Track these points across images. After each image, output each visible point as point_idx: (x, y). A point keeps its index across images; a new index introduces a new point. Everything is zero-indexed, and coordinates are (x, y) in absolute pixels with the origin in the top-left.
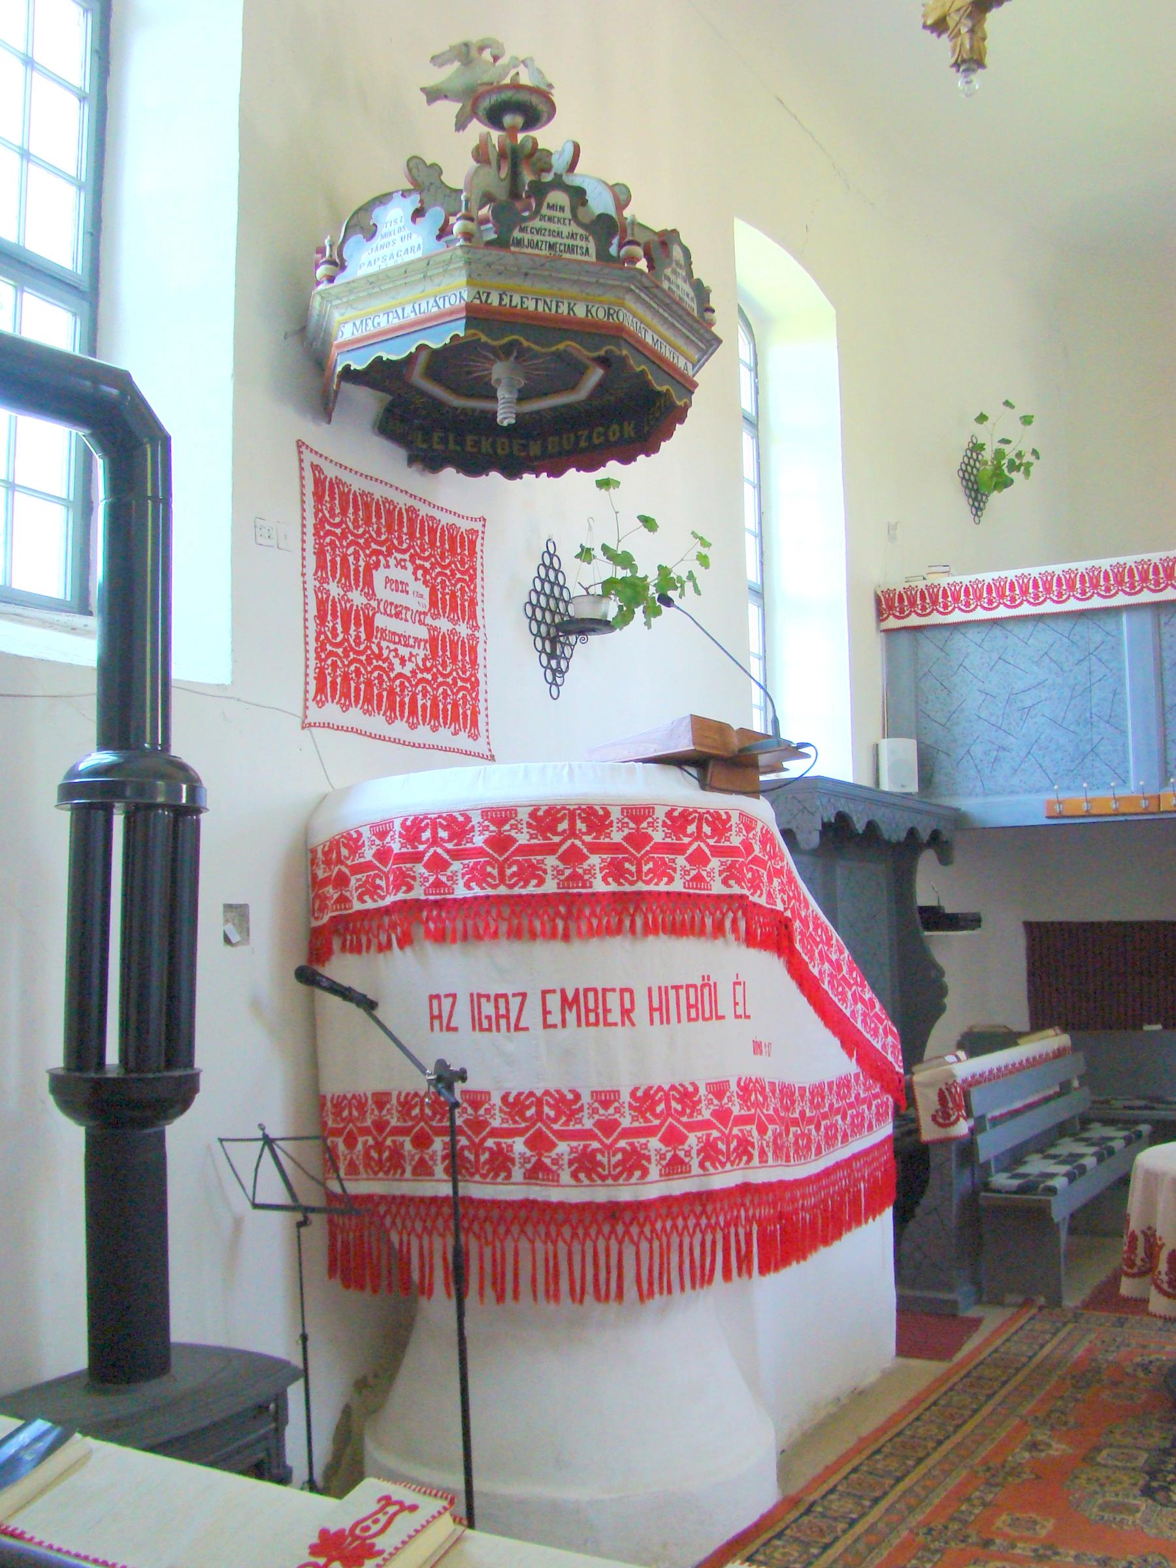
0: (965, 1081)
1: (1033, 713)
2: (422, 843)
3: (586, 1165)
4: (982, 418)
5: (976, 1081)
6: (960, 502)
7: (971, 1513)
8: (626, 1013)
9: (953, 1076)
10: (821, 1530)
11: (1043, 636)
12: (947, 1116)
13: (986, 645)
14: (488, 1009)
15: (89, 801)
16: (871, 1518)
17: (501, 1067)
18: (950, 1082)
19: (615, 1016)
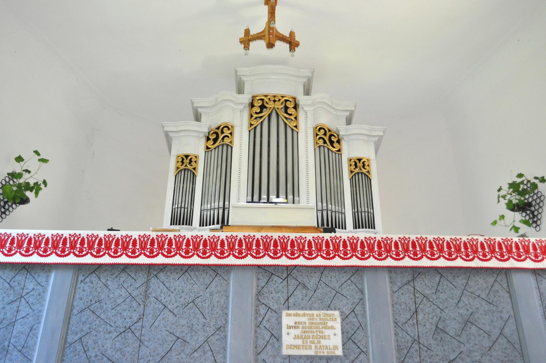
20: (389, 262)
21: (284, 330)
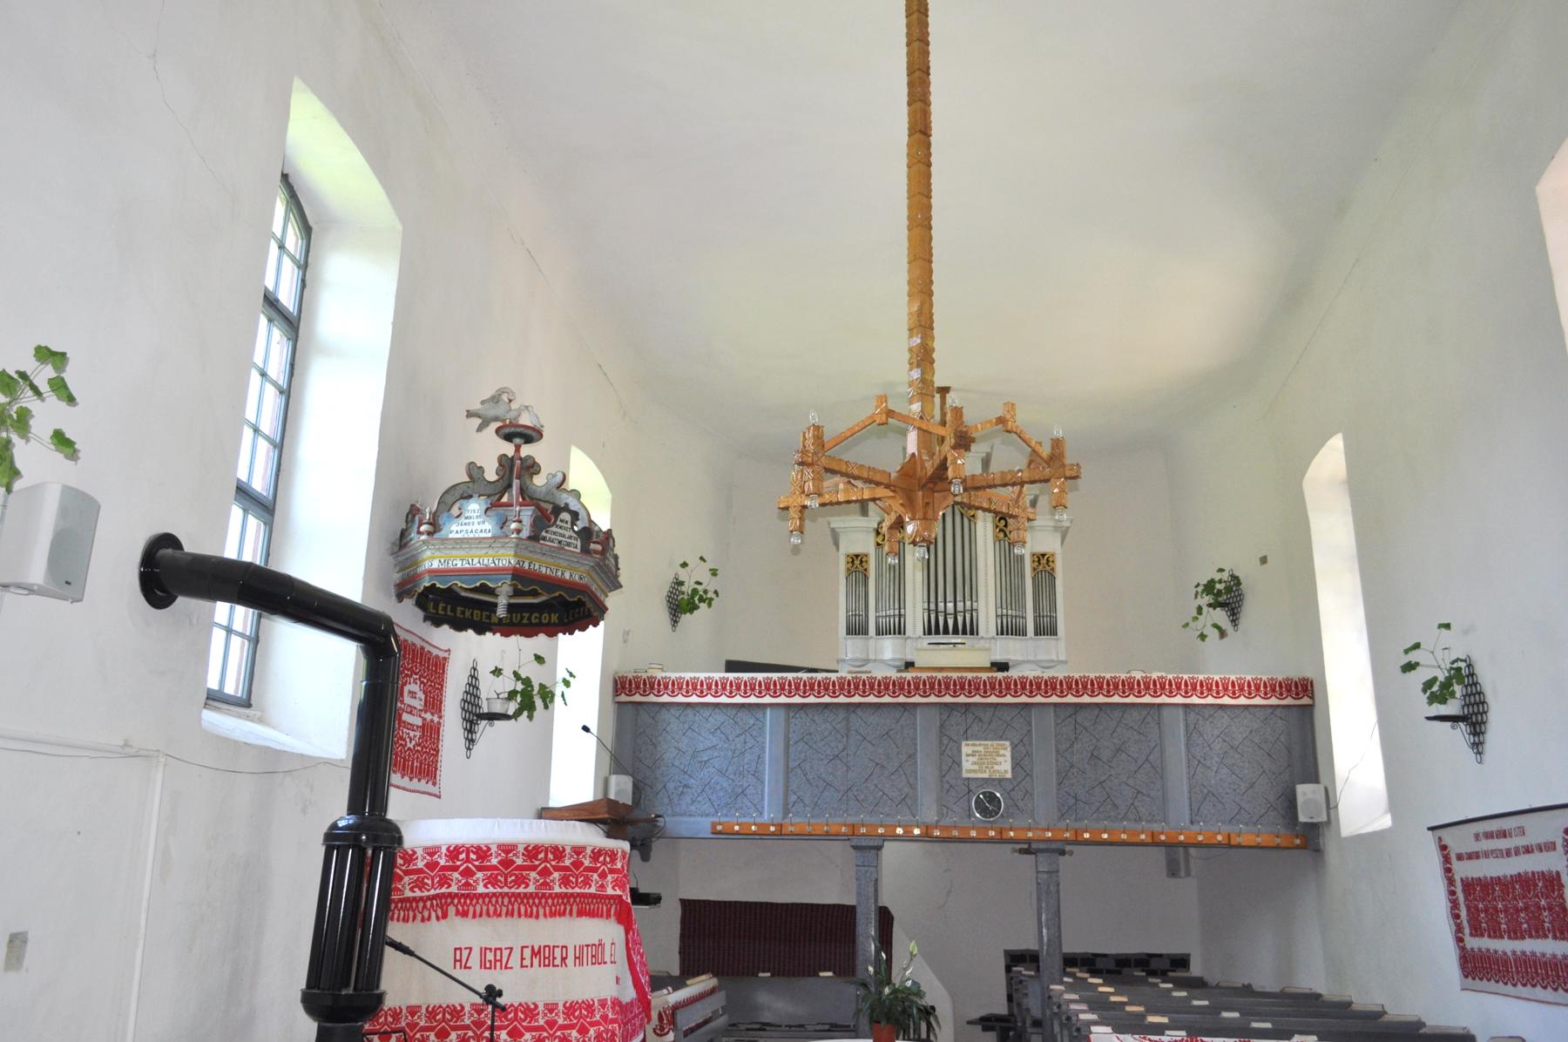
4: (684, 565)
5: (676, 1007)
6: (664, 615)
8: (564, 959)
11: (719, 717)
12: (662, 1029)
14: (490, 956)
15: (335, 840)
17: (517, 987)
19: (558, 962)
20: (1054, 699)
21: (964, 758)
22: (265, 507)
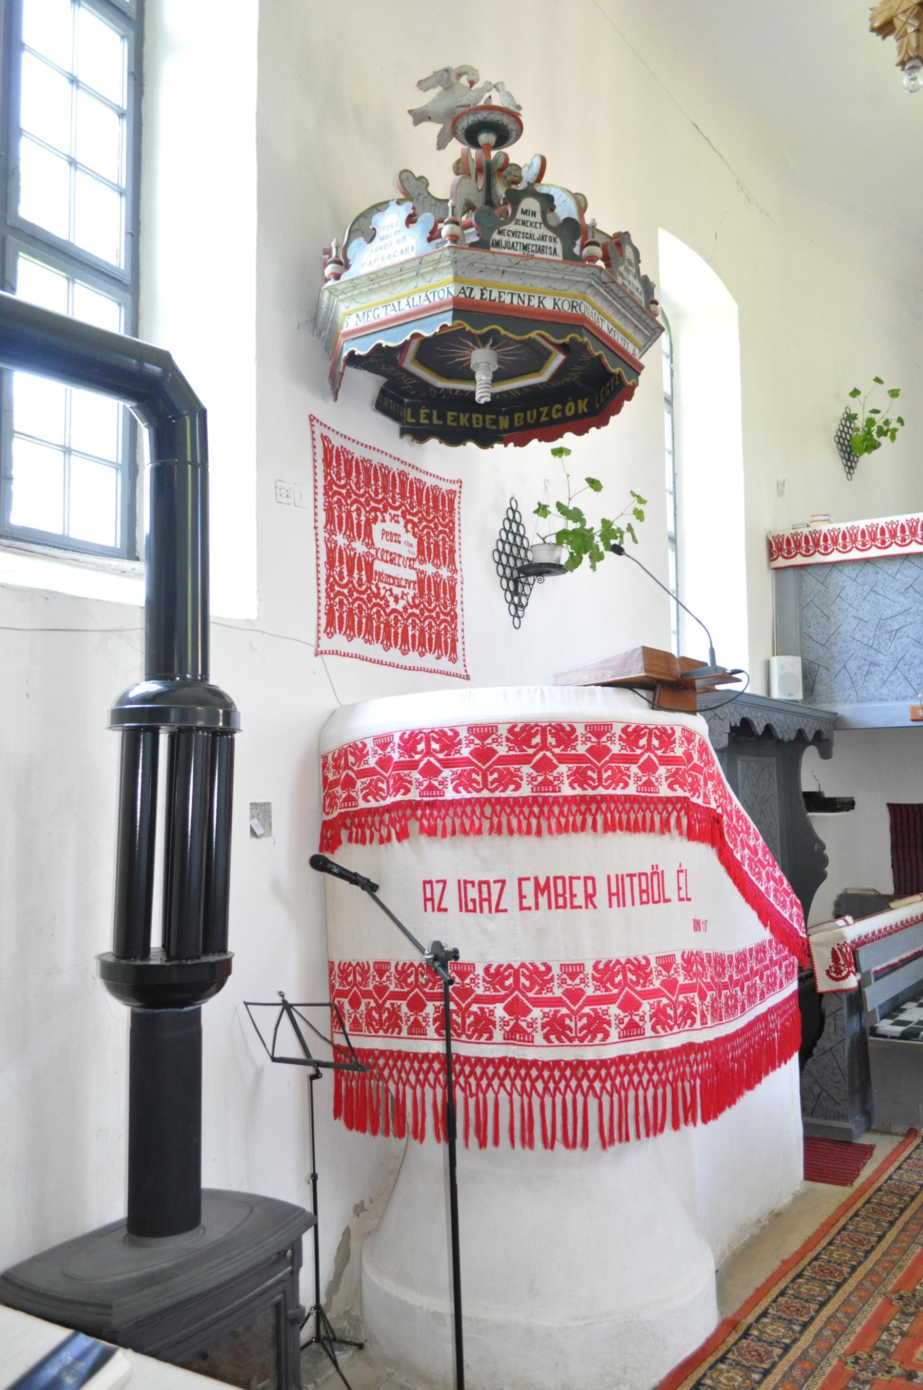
0: (853, 942)
1: (899, 634)
2: (417, 753)
3: (556, 1029)
4: (855, 393)
5: (861, 942)
6: (835, 462)
7: (891, 1343)
8: (589, 897)
9: (843, 937)
10: (760, 1355)
12: (838, 971)
13: (859, 580)
14: (473, 893)
15: (138, 724)
16: (803, 1343)
18: (841, 943)
19: (580, 900)
22: (129, 284)
